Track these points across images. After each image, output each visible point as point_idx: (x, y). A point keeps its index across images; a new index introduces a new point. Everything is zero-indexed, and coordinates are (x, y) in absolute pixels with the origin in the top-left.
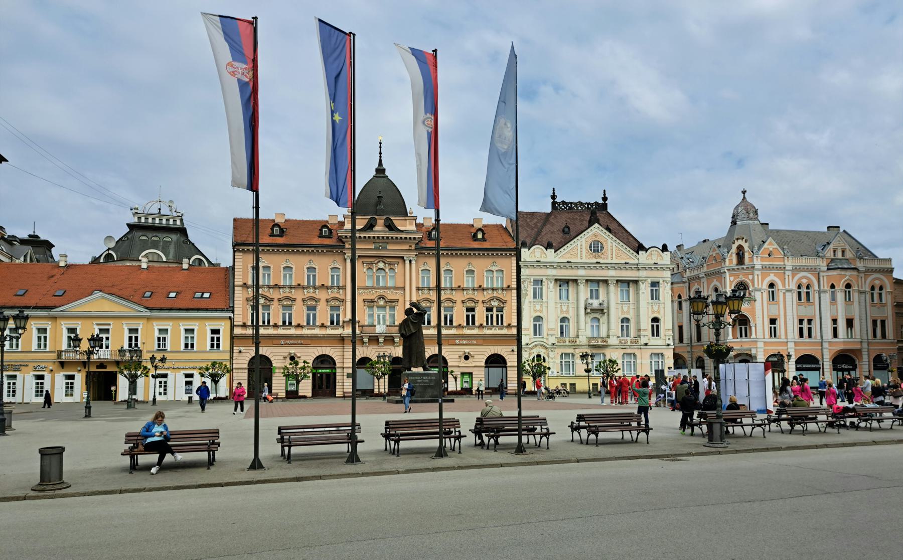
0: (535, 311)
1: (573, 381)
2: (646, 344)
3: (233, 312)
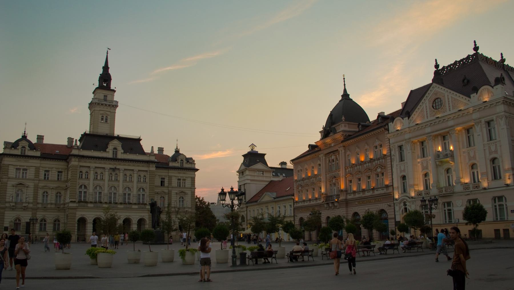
0: (401, 171)
2: (485, 189)
3: (293, 195)
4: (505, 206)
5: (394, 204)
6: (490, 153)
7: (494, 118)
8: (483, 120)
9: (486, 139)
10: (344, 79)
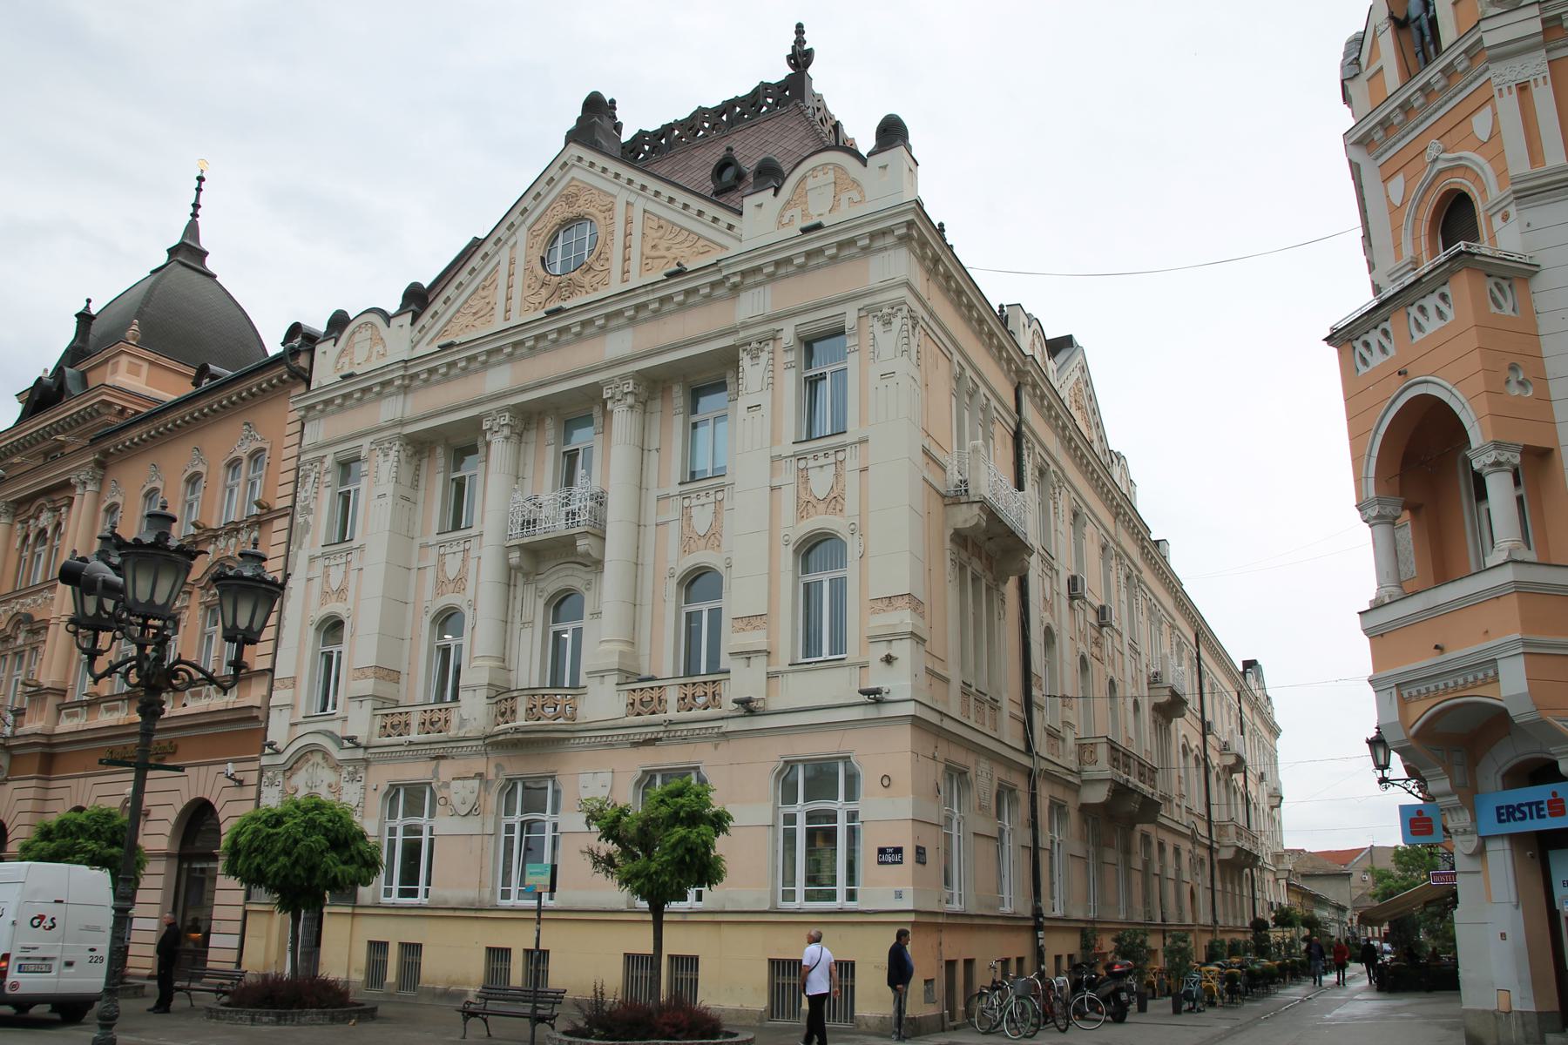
1: (410, 932)
2: (747, 707)
4: (842, 826)
5: (262, 771)
6: (804, 507)
7: (850, 321)
8: (788, 334)
9: (790, 425)
10: (201, 179)
